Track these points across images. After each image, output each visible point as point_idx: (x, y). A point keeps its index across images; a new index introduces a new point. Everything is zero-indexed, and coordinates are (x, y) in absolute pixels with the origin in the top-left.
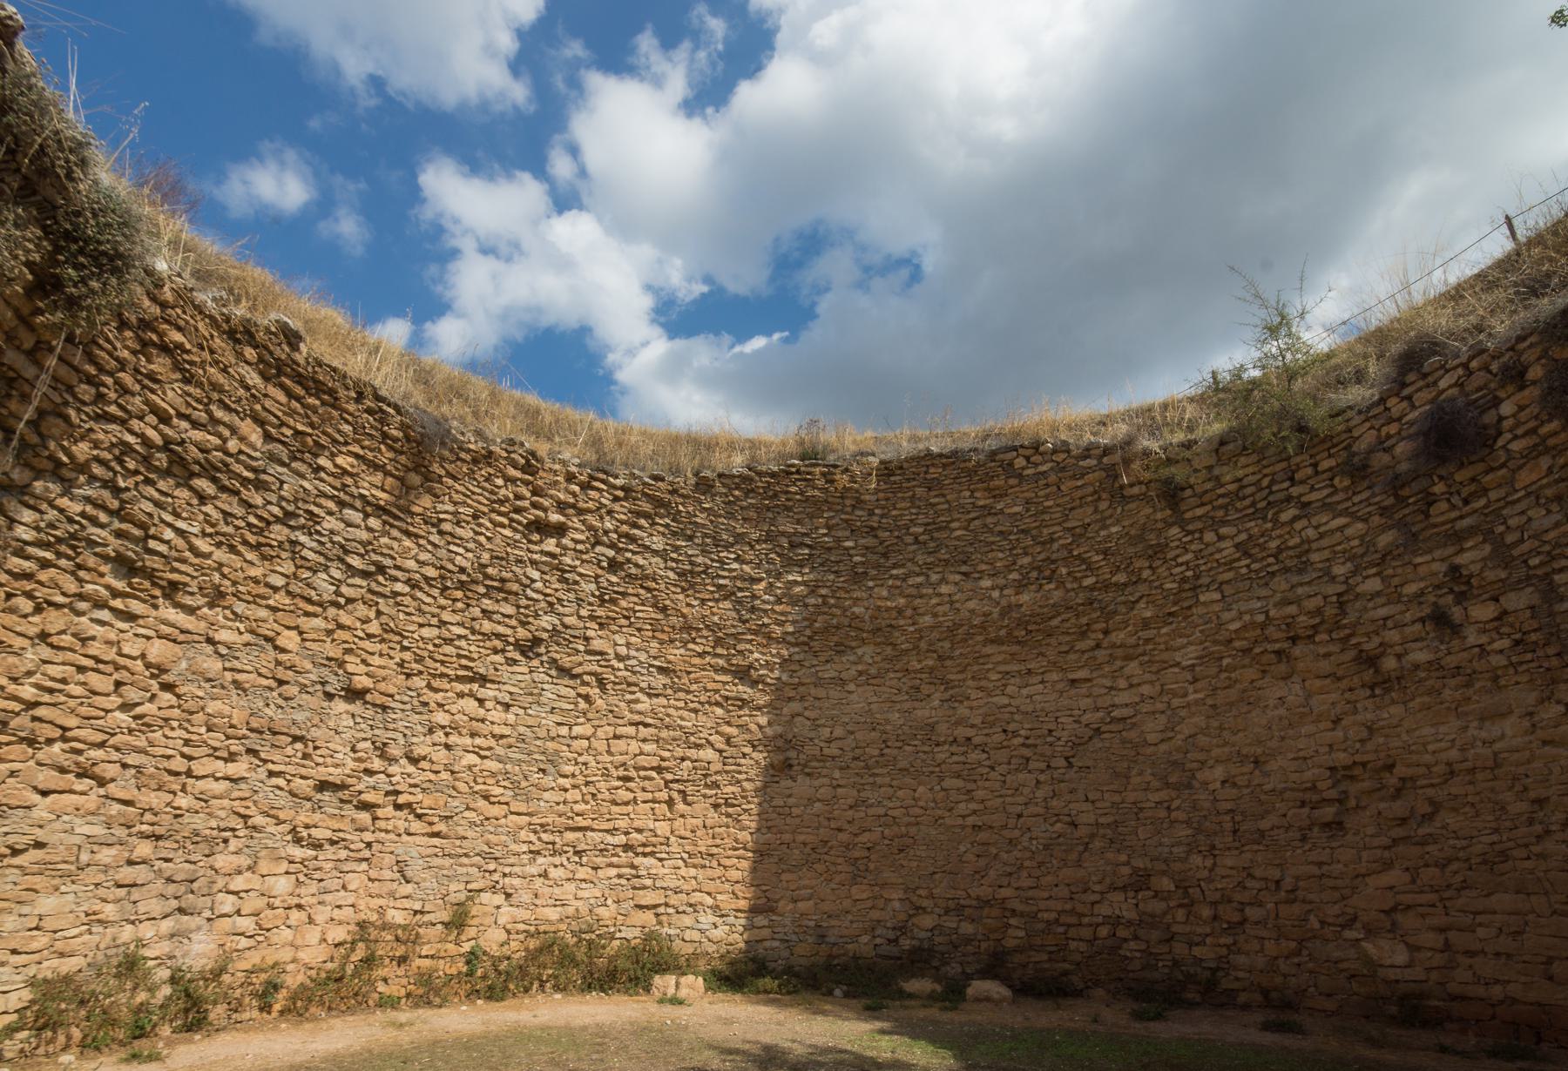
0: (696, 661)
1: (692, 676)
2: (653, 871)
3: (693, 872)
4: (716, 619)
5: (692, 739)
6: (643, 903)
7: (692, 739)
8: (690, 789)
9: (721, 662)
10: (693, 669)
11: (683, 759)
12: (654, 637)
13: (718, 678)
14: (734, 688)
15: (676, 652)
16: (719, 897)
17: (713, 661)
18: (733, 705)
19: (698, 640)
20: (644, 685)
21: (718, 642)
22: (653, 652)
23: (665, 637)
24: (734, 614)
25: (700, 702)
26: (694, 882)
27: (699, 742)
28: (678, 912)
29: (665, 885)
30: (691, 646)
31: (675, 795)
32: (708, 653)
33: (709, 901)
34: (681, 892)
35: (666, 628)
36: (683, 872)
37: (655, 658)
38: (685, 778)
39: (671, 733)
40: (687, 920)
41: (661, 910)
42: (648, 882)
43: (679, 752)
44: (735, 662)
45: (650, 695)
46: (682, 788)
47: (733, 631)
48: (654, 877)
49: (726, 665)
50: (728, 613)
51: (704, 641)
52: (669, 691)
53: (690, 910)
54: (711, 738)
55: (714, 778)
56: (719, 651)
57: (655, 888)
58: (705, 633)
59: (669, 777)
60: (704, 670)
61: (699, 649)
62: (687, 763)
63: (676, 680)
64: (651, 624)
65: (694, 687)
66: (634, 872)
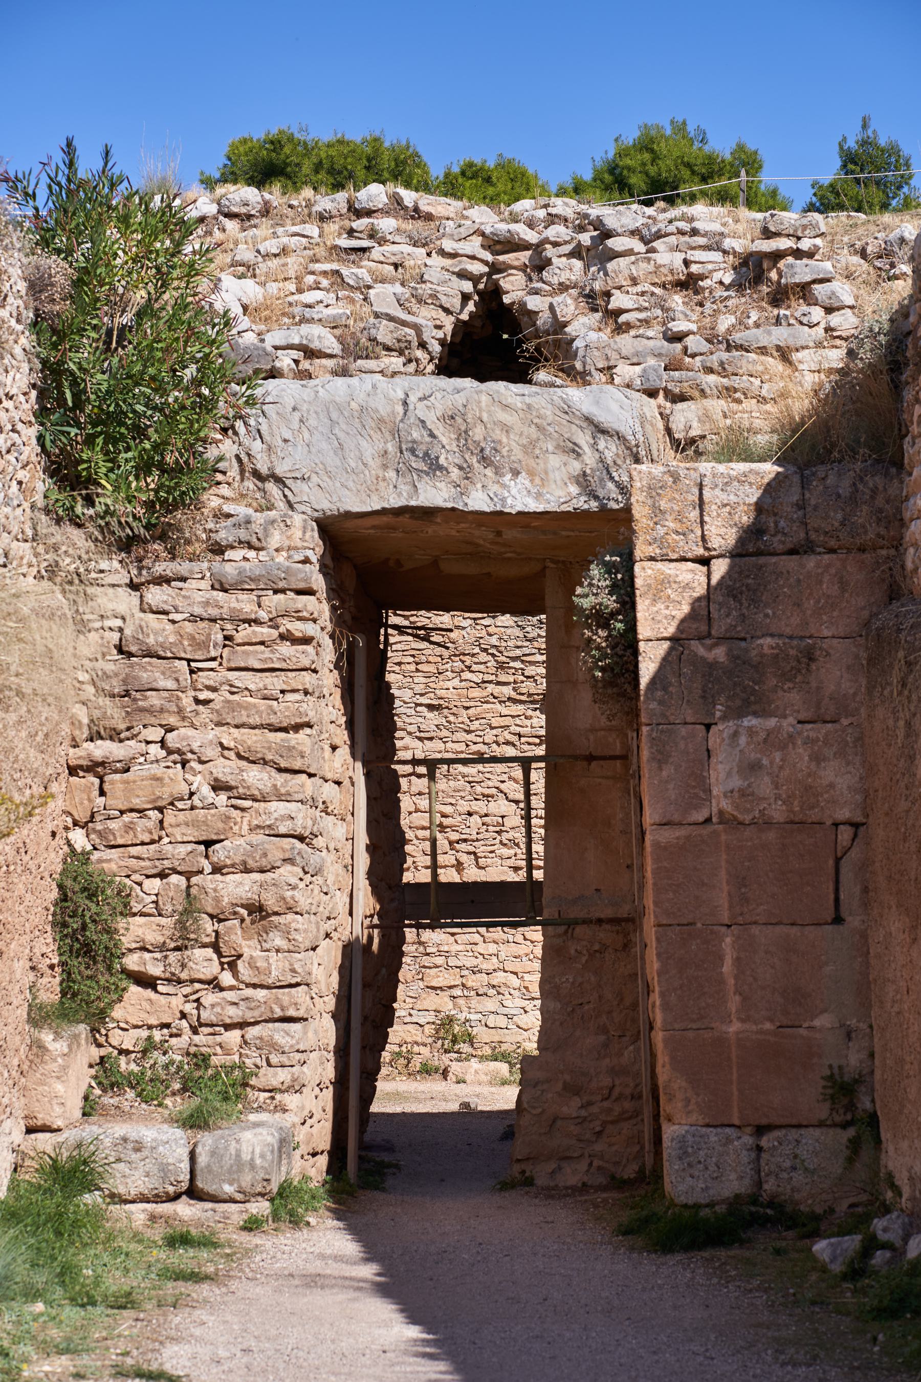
0: (476, 693)
1: (471, 712)
2: (446, 948)
3: (492, 948)
4: (494, 640)
5: (479, 789)
6: (434, 984)
7: (479, 789)
8: (481, 850)
9: (507, 691)
10: (472, 704)
11: (470, 814)
12: (417, 670)
13: (505, 711)
14: (528, 722)
15: (449, 684)
16: (527, 977)
17: (497, 690)
18: (529, 744)
19: (475, 667)
20: (411, 728)
21: (501, 666)
22: (419, 689)
23: (432, 668)
24: (517, 632)
25: (484, 743)
26: (494, 959)
27: (487, 791)
28: (478, 995)
29: (460, 964)
30: (467, 675)
31: (464, 858)
32: (490, 682)
33: (514, 981)
34: (480, 972)
35: (431, 659)
36: (481, 948)
37: (422, 695)
38: (474, 837)
39: (451, 783)
40: (490, 1004)
41: (457, 992)
42: (440, 961)
43: (464, 806)
44: (524, 691)
45: (420, 739)
46: (471, 849)
47: (518, 652)
48: (447, 955)
49: (513, 695)
50: (509, 631)
51: (482, 667)
52: (445, 733)
53: (492, 992)
54: (503, 786)
55: (510, 835)
56: (503, 678)
57: (448, 967)
58: (483, 657)
59: (454, 836)
60: (487, 702)
61: (477, 678)
62: (475, 820)
63: (452, 718)
64: (413, 656)
65: (476, 725)
66: (421, 949)
